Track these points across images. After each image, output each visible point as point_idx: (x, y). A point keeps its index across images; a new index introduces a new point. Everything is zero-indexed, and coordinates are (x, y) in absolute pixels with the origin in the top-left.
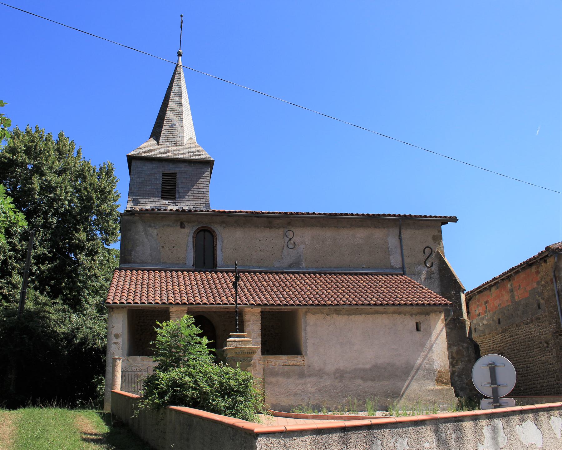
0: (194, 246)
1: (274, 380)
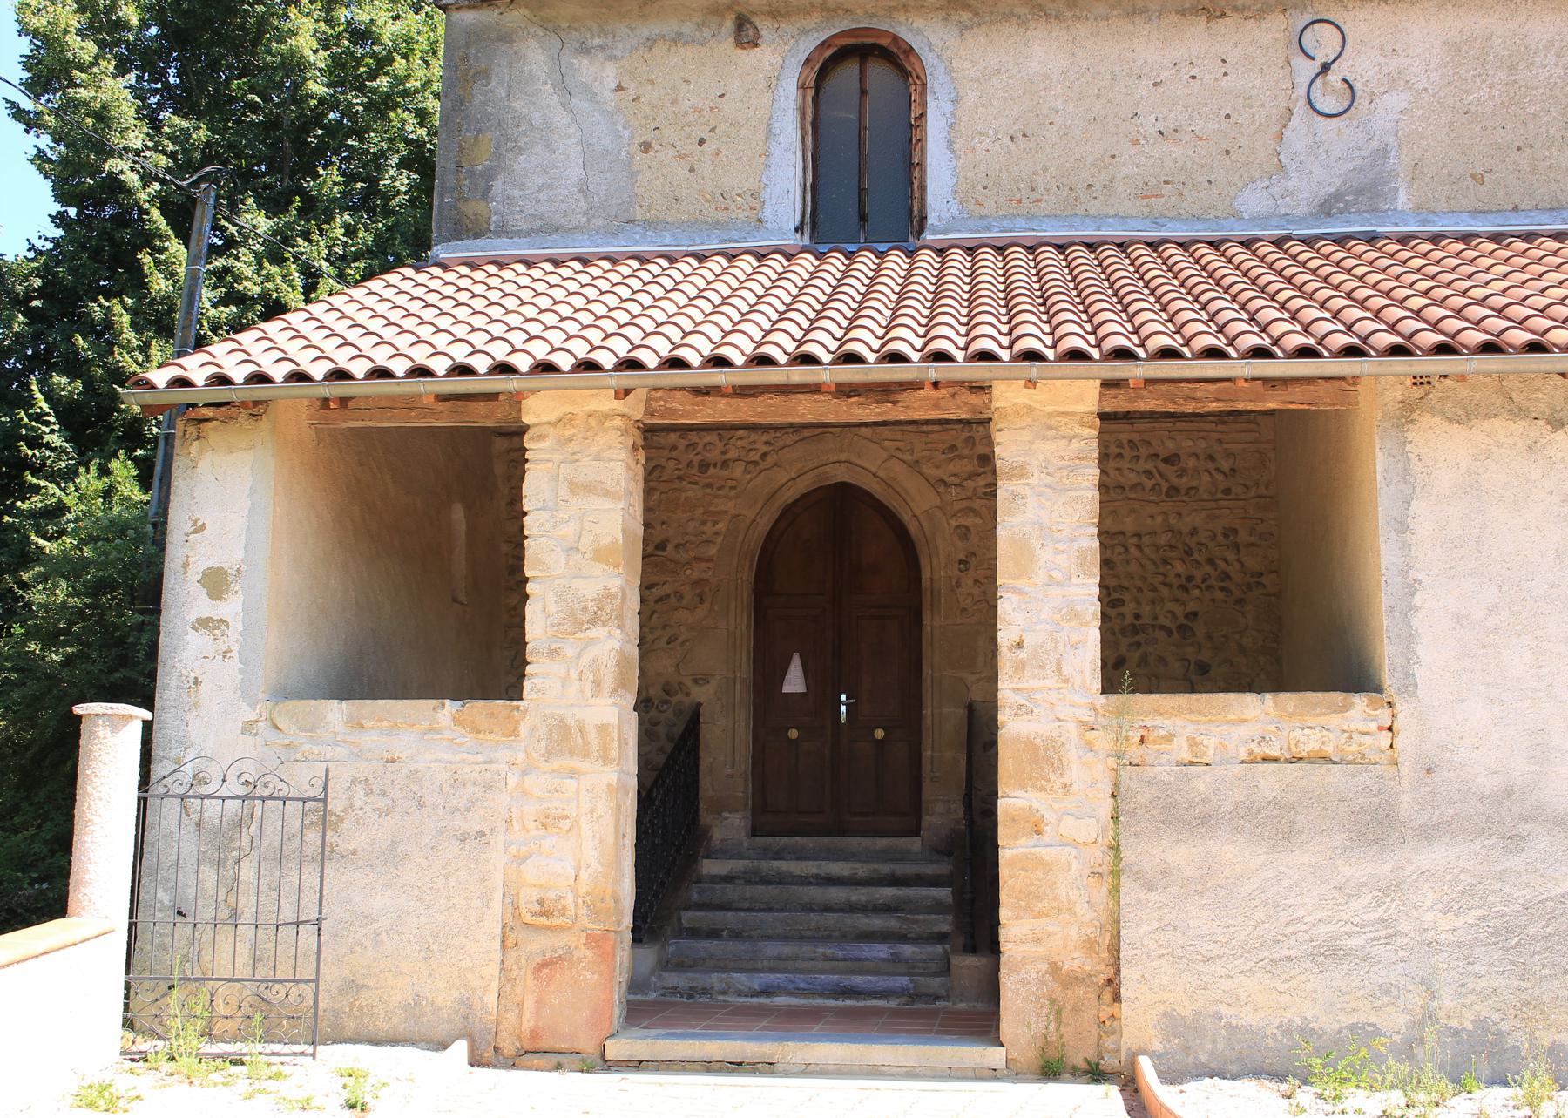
0: (803, 128)
1: (1181, 855)
